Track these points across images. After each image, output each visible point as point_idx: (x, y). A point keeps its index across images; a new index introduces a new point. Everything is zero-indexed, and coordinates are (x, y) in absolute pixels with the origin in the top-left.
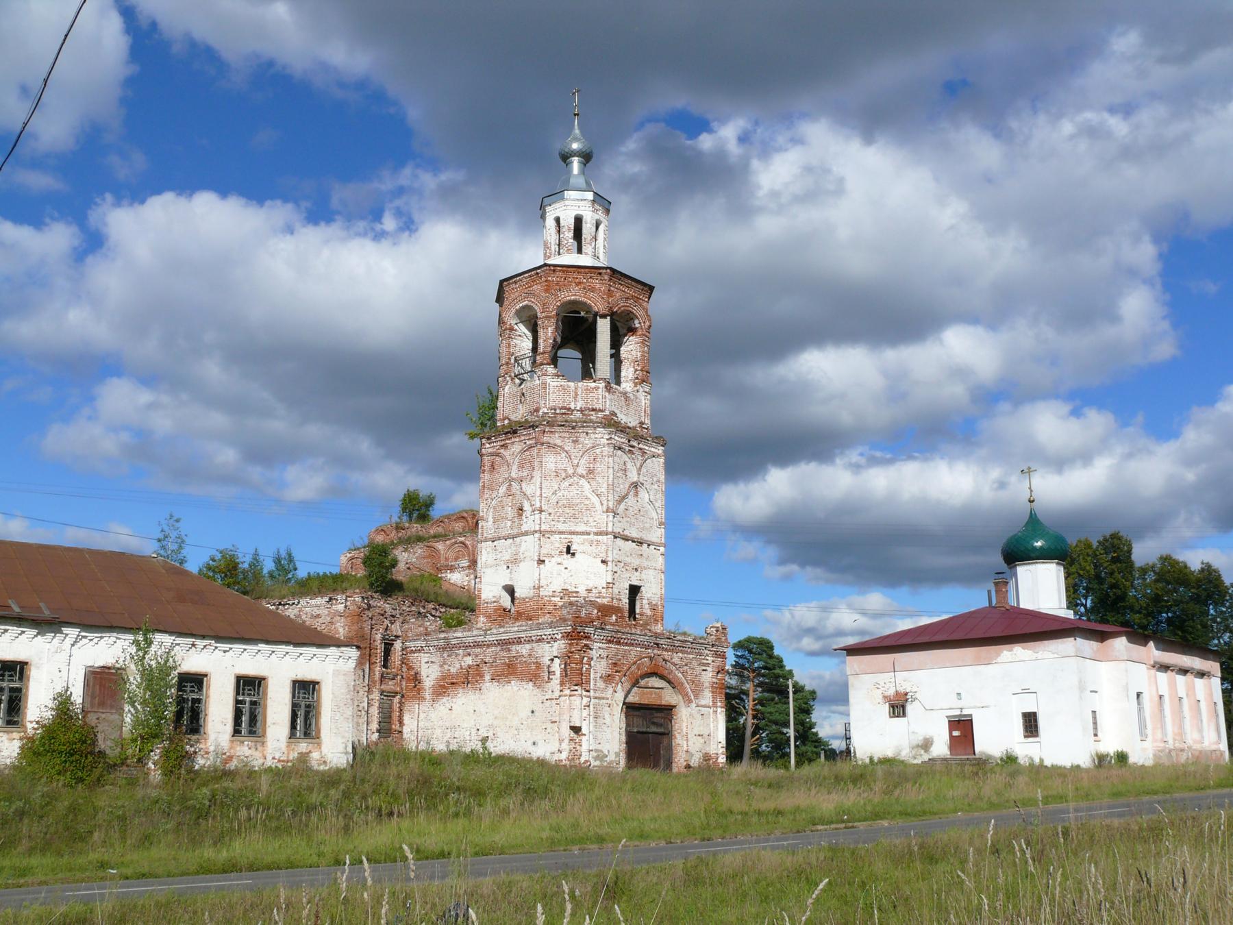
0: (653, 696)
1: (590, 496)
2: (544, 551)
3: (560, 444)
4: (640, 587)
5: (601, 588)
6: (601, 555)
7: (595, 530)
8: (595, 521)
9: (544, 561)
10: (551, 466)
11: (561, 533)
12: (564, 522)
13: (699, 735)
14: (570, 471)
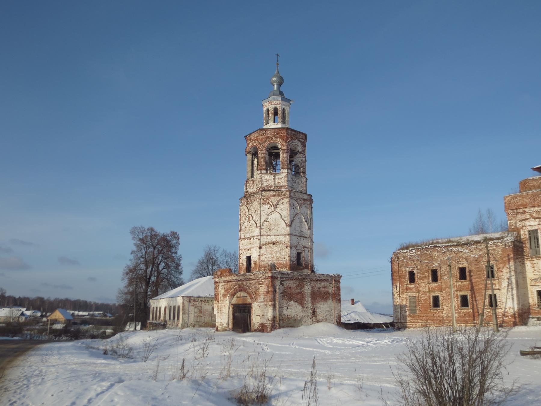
13: (258, 315)
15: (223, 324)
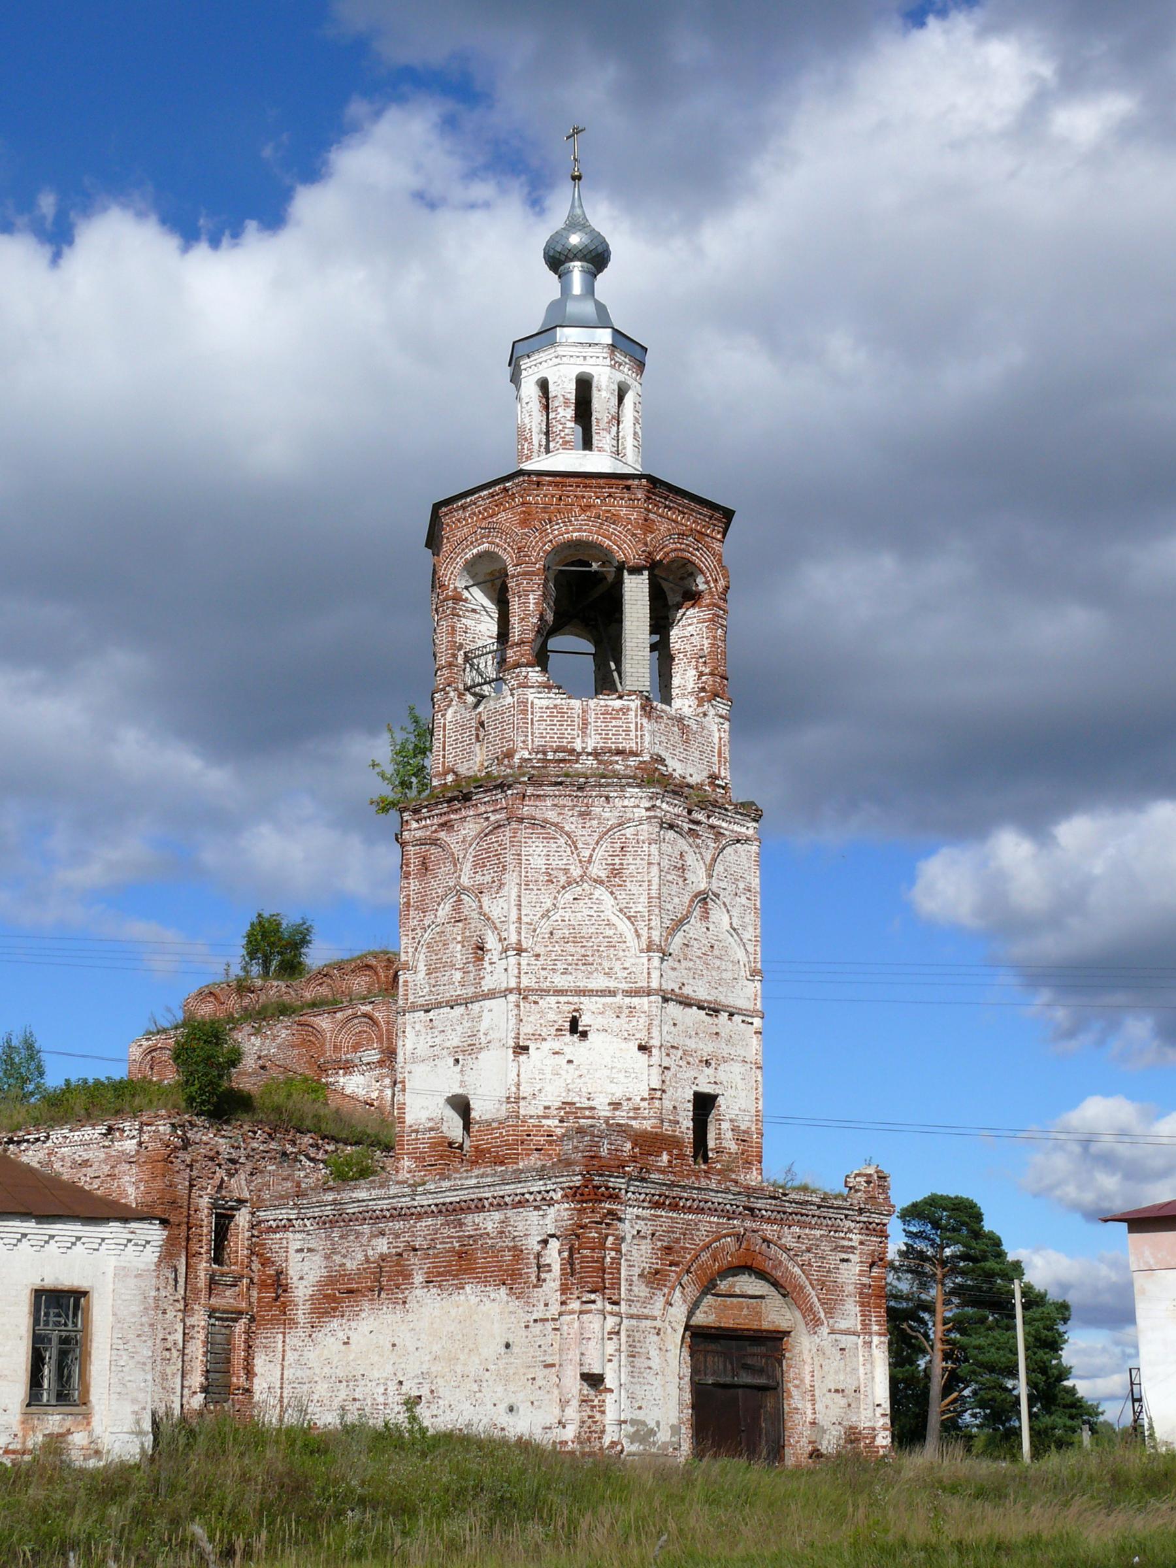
0: (745, 1312)
1: (614, 919)
2: (526, 1029)
3: (556, 820)
4: (715, 1097)
5: (638, 1098)
6: (638, 1036)
7: (625, 986)
8: (625, 969)
9: (526, 1048)
10: (539, 862)
11: (559, 992)
12: (565, 972)
13: (837, 1391)
14: (576, 872)
15: (652, 1433)
